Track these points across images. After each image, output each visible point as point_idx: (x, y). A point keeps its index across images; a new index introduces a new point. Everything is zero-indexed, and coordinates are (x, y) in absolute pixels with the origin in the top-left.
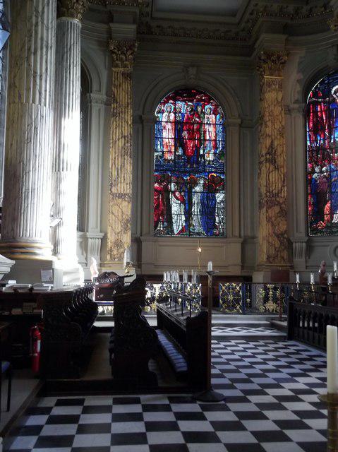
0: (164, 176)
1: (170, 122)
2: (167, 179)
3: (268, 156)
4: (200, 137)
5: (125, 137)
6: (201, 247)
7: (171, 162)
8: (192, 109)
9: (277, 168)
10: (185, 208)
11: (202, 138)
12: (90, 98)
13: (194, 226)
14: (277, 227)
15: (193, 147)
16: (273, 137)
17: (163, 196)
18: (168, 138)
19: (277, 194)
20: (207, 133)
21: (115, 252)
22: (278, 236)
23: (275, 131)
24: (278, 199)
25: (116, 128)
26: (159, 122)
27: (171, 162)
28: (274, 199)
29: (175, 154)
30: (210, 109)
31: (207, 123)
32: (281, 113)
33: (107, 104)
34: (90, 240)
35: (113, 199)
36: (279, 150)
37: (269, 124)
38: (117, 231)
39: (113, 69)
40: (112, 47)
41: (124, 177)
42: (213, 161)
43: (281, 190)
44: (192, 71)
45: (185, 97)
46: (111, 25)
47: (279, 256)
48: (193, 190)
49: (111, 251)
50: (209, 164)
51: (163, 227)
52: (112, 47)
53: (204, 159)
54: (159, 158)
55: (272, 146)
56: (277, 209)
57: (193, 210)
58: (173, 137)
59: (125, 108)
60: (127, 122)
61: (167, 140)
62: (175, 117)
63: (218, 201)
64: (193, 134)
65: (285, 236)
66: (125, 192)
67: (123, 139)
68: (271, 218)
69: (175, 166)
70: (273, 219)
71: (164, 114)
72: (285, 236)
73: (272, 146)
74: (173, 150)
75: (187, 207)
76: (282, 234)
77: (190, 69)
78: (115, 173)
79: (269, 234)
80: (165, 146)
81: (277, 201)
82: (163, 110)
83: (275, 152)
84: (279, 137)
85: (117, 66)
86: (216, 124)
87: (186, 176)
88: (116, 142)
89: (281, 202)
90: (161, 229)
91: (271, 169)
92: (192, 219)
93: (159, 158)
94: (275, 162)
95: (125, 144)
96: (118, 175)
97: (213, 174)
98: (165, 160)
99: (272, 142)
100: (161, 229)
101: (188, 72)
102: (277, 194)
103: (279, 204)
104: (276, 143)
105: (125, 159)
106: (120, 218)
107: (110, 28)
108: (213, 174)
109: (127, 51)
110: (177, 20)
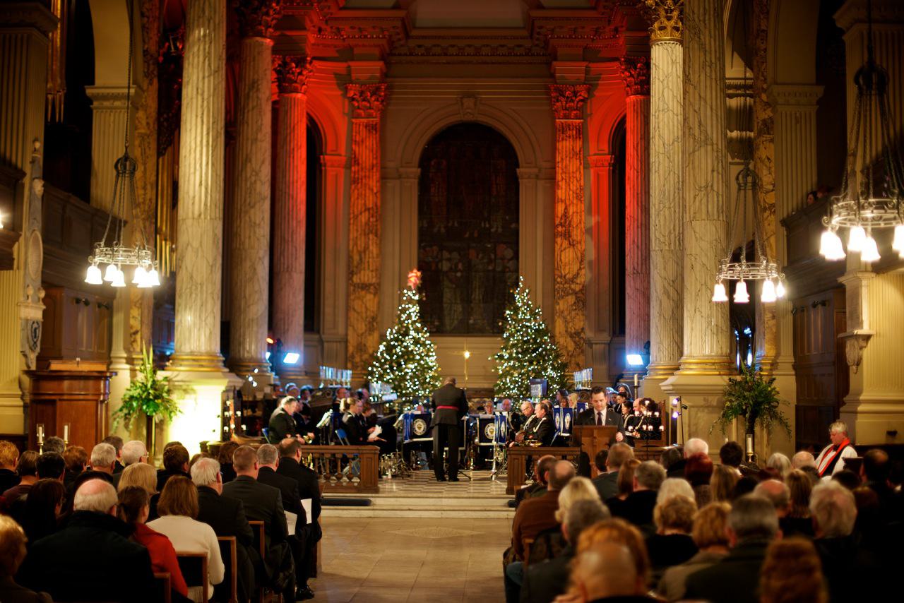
3: (560, 229)
5: (369, 209)
6: (469, 349)
9: (572, 245)
12: (324, 159)
14: (571, 325)
16: (568, 203)
19: (572, 280)
21: (357, 359)
22: (571, 336)
23: (571, 193)
24: (573, 286)
25: (358, 198)
28: (566, 286)
32: (579, 168)
33: (348, 167)
34: (326, 345)
35: (354, 290)
36: (576, 220)
37: (562, 184)
38: (360, 332)
39: (354, 120)
40: (351, 94)
41: (368, 262)
43: (578, 274)
44: (469, 103)
46: (351, 63)
47: (573, 362)
49: (353, 357)
52: (351, 94)
55: (565, 214)
56: (571, 299)
57: (473, 297)
59: (369, 171)
60: (372, 190)
65: (582, 335)
66: (370, 282)
67: (367, 213)
68: (562, 312)
70: (566, 313)
72: (582, 335)
73: (565, 214)
76: (578, 334)
77: (465, 100)
78: (356, 257)
79: (560, 333)
81: (572, 290)
83: (570, 222)
84: (575, 202)
85: (359, 116)
88: (357, 216)
89: (577, 289)
91: (564, 246)
94: (570, 236)
95: (369, 218)
96: (361, 259)
99: (566, 208)
101: (462, 104)
102: (572, 280)
103: (575, 293)
104: (571, 211)
105: (369, 239)
106: (364, 315)
107: (349, 66)
109: (371, 96)
110: (443, 37)
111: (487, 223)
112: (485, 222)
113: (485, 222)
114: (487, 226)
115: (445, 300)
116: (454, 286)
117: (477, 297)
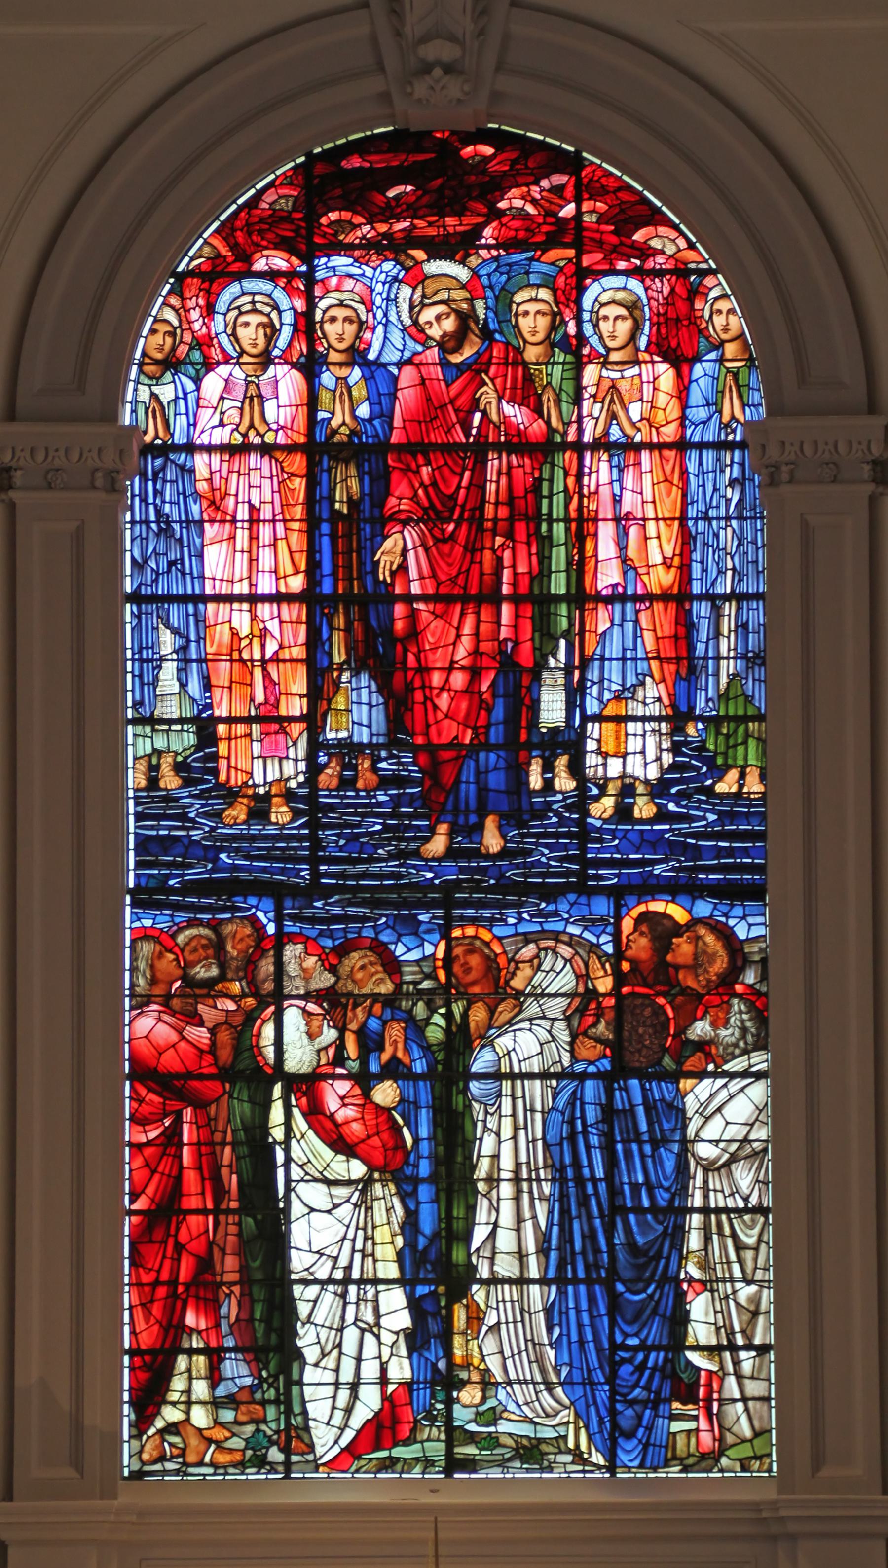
0: (218, 947)
1: (266, 450)
2: (249, 965)
4: (543, 573)
7: (280, 814)
8: (465, 319)
10: (410, 1225)
11: (559, 585)
13: (487, 1383)
15: (474, 673)
17: (204, 1124)
18: (253, 599)
20: (606, 532)
26: (165, 450)
27: (280, 814)
29: (314, 746)
30: (633, 307)
31: (602, 444)
42: (658, 789)
45: (391, 211)
48: (482, 1061)
50: (623, 812)
51: (215, 1404)
53: (576, 769)
54: (170, 781)
57: (480, 1234)
58: (296, 583)
61: (241, 620)
62: (312, 402)
63: (705, 1151)
64: (473, 549)
69: (316, 844)
71: (212, 384)
74: (296, 707)
75: (427, 1222)
80: (223, 672)
82: (204, 343)
86: (682, 446)
87: (412, 927)
90: (200, 1417)
92: (476, 1318)
93: (170, 781)
97: (657, 906)
98: (231, 795)
100: (200, 1417)
108: (657, 906)
111: (562, 762)
112: (548, 767)
113: (548, 767)
114: (564, 783)
115: (299, 1261)
116: (358, 1169)
117: (506, 1241)
